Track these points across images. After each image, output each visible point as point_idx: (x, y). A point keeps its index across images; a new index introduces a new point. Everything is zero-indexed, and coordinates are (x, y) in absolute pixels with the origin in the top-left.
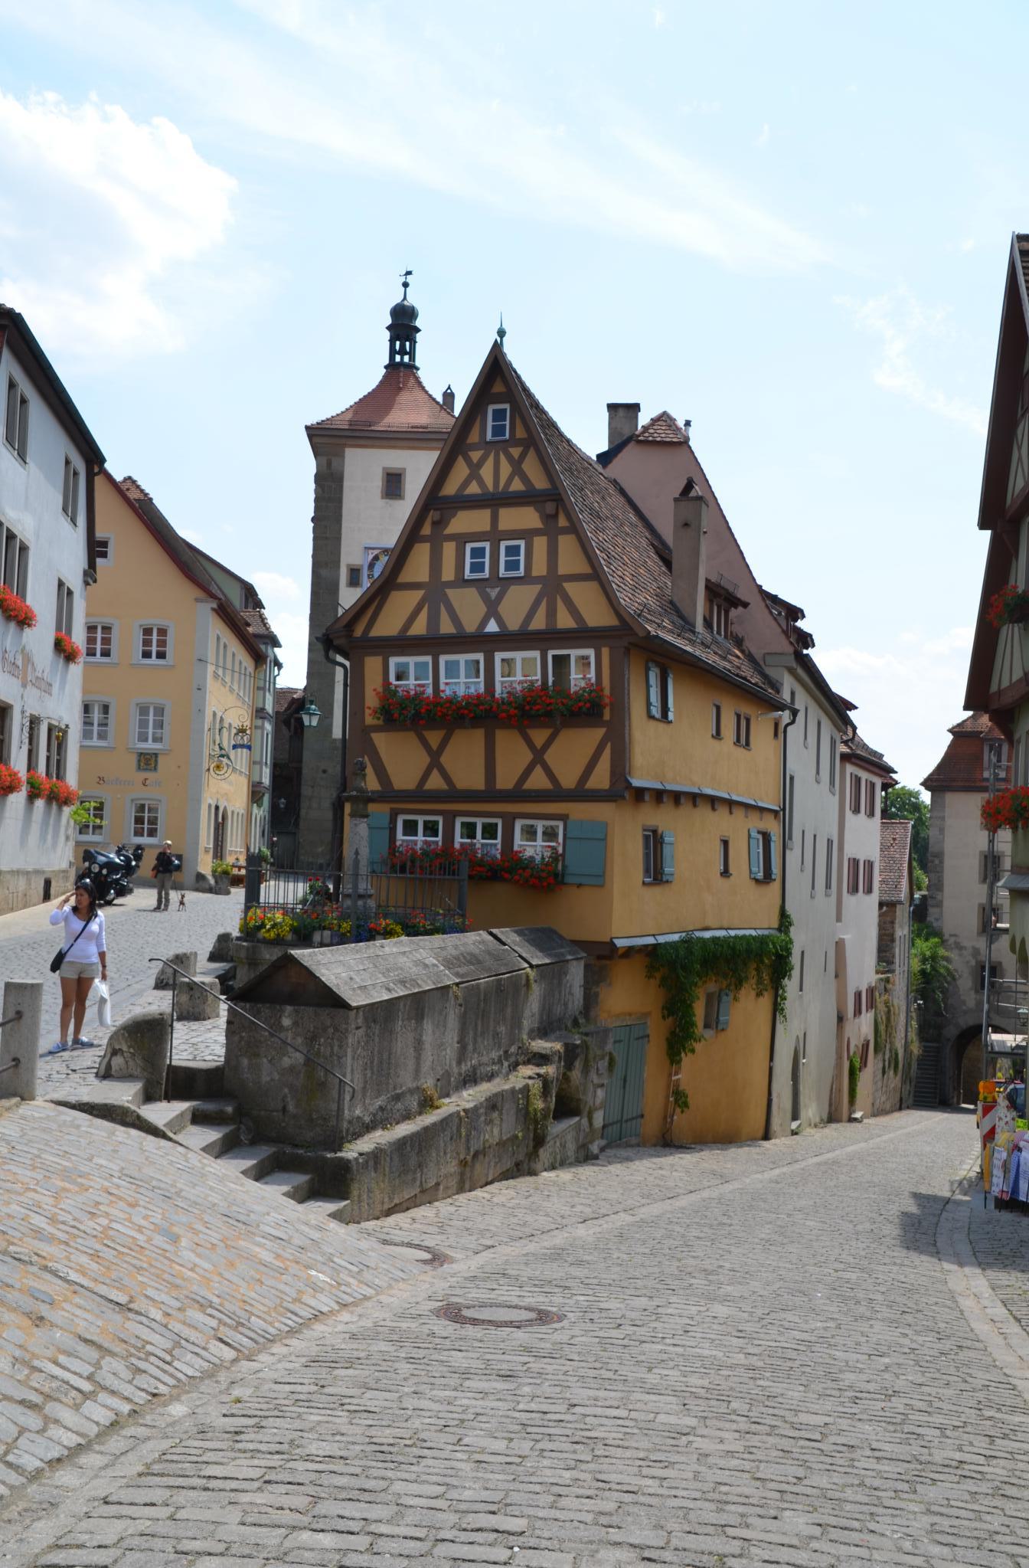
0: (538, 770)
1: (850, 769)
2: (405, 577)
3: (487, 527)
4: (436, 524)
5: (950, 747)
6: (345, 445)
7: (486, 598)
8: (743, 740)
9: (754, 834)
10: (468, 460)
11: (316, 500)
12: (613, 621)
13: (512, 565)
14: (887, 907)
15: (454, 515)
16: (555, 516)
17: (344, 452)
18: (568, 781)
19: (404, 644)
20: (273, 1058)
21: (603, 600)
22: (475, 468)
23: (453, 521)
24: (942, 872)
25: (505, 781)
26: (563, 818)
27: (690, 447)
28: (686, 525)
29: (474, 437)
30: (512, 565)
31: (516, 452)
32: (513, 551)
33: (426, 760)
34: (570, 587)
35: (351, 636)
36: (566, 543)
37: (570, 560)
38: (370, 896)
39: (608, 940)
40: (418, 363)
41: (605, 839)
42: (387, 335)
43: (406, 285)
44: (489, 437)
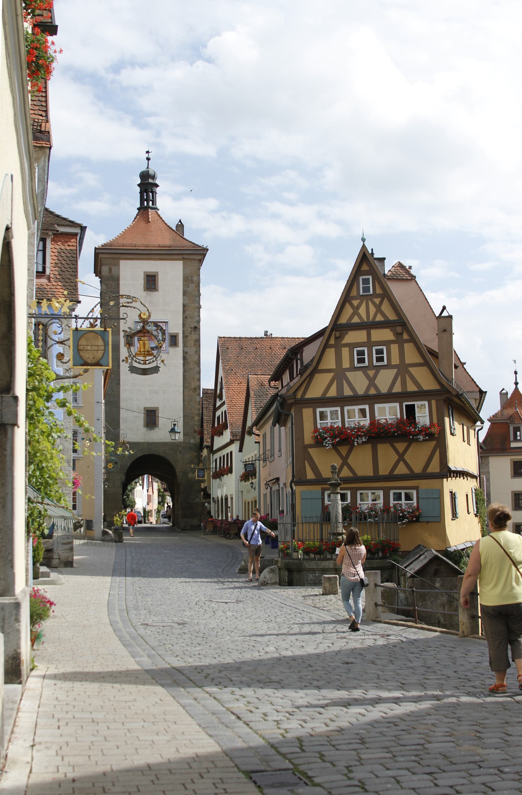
0: (401, 463)
2: (321, 367)
3: (365, 340)
4: (336, 338)
5: (489, 429)
7: (367, 376)
9: (474, 491)
12: (436, 387)
16: (402, 334)
18: (418, 469)
19: (325, 401)
21: (431, 377)
22: (356, 309)
23: (346, 336)
25: (384, 470)
26: (416, 488)
27: (416, 282)
28: (445, 330)
29: (354, 293)
31: (377, 301)
35: (295, 398)
36: (409, 347)
38: (344, 533)
39: (444, 549)
40: (158, 208)
41: (439, 498)
42: (138, 189)
43: (148, 159)
44: (361, 293)
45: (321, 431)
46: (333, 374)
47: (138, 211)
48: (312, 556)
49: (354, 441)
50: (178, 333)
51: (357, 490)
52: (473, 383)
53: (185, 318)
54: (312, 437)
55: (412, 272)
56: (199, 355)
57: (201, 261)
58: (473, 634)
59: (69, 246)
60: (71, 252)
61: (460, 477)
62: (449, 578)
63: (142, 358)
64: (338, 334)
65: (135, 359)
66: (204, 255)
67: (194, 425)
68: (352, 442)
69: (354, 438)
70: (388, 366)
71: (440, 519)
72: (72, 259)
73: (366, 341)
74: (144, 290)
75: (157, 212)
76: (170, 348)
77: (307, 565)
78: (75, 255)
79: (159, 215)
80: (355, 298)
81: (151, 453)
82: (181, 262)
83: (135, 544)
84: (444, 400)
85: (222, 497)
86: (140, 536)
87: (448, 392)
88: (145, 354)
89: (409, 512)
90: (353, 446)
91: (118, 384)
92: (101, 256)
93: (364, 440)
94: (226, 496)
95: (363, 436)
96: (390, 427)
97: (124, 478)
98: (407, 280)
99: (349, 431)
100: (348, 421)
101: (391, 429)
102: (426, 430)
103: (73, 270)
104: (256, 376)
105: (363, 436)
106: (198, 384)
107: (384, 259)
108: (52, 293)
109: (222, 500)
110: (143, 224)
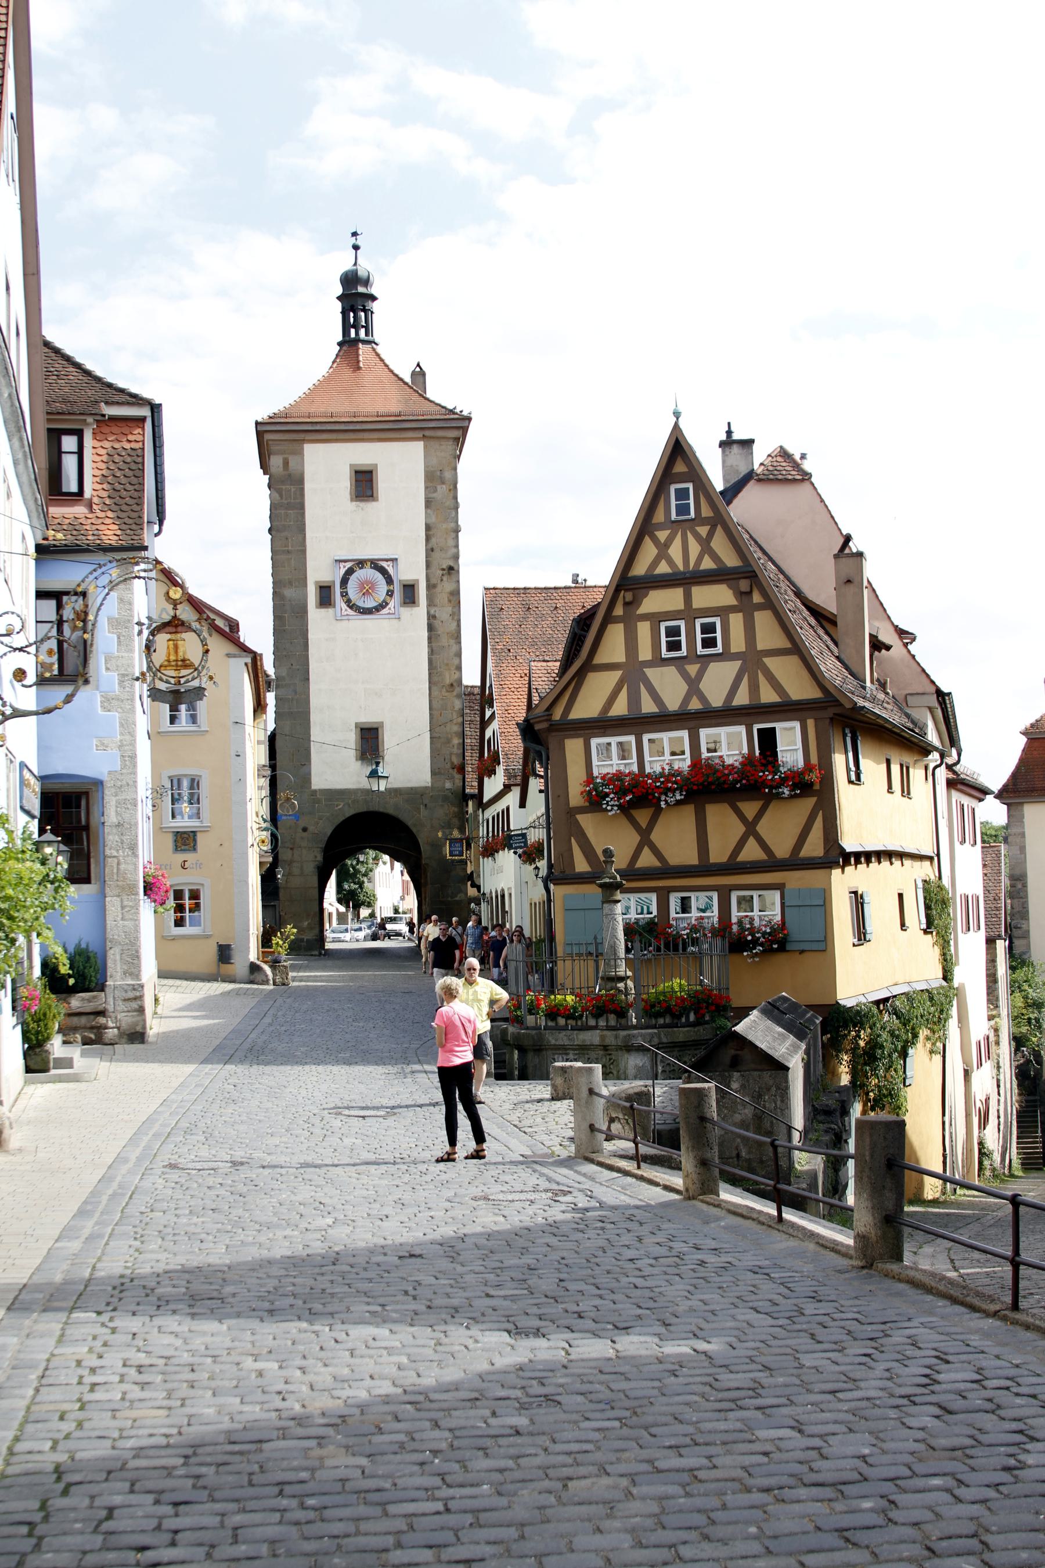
1: (956, 795)
2: (600, 659)
3: (681, 607)
4: (626, 604)
6: (304, 441)
7: (685, 675)
8: (906, 792)
9: (920, 885)
10: (655, 541)
11: (273, 507)
13: (708, 643)
14: (990, 942)
15: (646, 595)
16: (750, 593)
17: (303, 449)
18: (782, 850)
19: (604, 725)
20: (725, 1116)
21: (805, 673)
22: (663, 549)
24: (1026, 897)
25: (718, 854)
26: (780, 887)
27: (812, 484)
28: (849, 581)
29: (659, 517)
30: (708, 643)
31: (703, 531)
32: (708, 629)
33: (636, 838)
34: (769, 662)
35: (550, 720)
36: (763, 620)
37: (768, 635)
40: (377, 337)
41: (824, 905)
42: (338, 306)
43: (356, 248)
44: (674, 516)
45: (599, 780)
46: (621, 672)
47: (338, 348)
48: (562, 1021)
49: (659, 800)
50: (418, 580)
51: (669, 892)
52: (924, 676)
53: (430, 551)
54: (582, 793)
55: (807, 466)
56: (459, 621)
57: (459, 441)
58: (704, 1194)
59: (129, 441)
60: (132, 453)
61: (879, 862)
62: (756, 1073)
63: (173, 673)
64: (629, 597)
65: (159, 674)
66: (465, 430)
67: (451, 754)
68: (654, 801)
69: (661, 794)
70: (725, 656)
71: (824, 945)
72: (133, 466)
73: (682, 607)
74: (352, 500)
75: (374, 350)
76: (402, 609)
77: (554, 1039)
78: (140, 460)
79: (378, 355)
80: (661, 527)
81: (371, 809)
82: (420, 444)
83: (316, 988)
84: (832, 719)
85: (496, 892)
86: (353, 969)
87: (837, 703)
88: (177, 666)
89: (764, 934)
90: (659, 810)
91: (307, 679)
92: (267, 437)
93: (678, 797)
94: (503, 890)
95: (676, 789)
96: (726, 772)
97: (320, 858)
98: (795, 481)
99: (650, 781)
100: (650, 762)
101: (728, 775)
102: (793, 777)
103: (136, 487)
104: (544, 664)
105: (676, 789)
106: (456, 676)
107: (752, 441)
108: (96, 532)
109: (497, 897)
110: (347, 373)
